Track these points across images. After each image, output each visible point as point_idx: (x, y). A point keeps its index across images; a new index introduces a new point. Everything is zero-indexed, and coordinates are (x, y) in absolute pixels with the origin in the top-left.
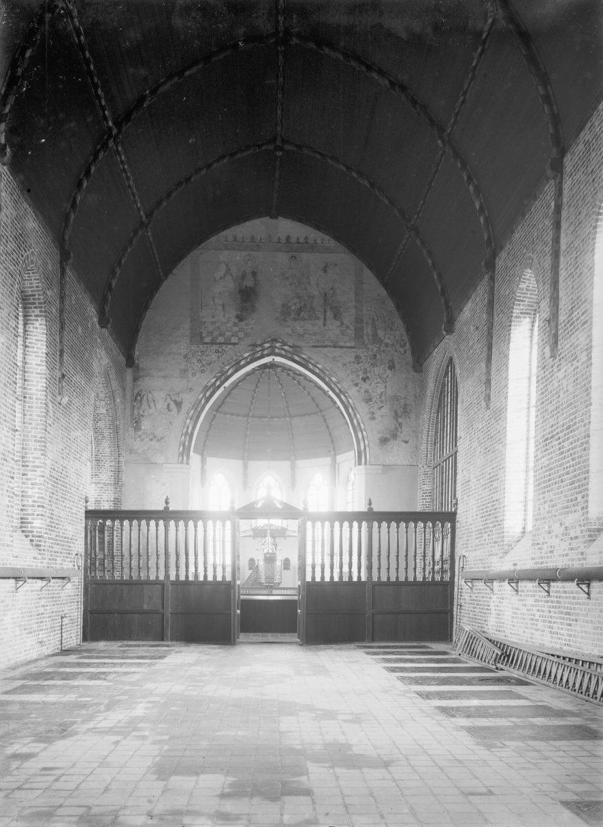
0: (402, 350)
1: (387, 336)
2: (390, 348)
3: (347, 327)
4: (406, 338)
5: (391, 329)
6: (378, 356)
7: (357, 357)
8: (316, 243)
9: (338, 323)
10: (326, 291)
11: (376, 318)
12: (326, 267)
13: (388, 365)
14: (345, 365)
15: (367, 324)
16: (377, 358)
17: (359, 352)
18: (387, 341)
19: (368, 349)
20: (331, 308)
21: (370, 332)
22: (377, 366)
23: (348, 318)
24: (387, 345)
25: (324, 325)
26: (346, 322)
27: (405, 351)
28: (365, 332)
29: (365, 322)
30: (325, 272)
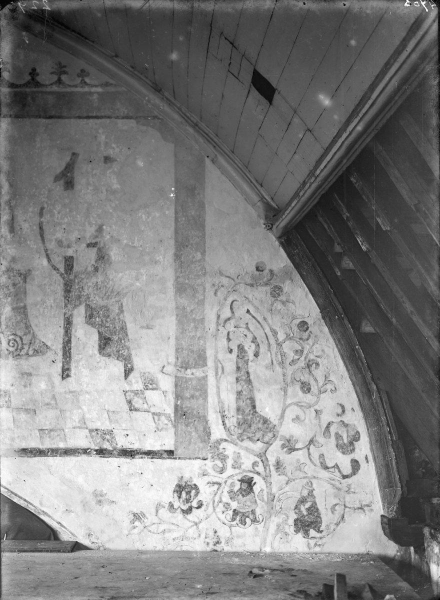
0: (345, 462)
1: (291, 413)
2: (301, 455)
3: (150, 384)
4: (357, 419)
5: (306, 388)
6: (259, 484)
7: (184, 489)
8: (38, 84)
9: (117, 367)
10: (70, 252)
11: (250, 349)
12: (69, 168)
13: (293, 516)
14: (137, 517)
15: (220, 370)
16: (256, 489)
17: (190, 469)
18: (289, 429)
19: (223, 458)
20: (90, 318)
21: (230, 399)
22: (254, 521)
23: (154, 353)
24: (290, 446)
25: (65, 373)
26: (143, 362)
27: (356, 465)
28: (212, 399)
29: (210, 363)
30: (69, 185)
